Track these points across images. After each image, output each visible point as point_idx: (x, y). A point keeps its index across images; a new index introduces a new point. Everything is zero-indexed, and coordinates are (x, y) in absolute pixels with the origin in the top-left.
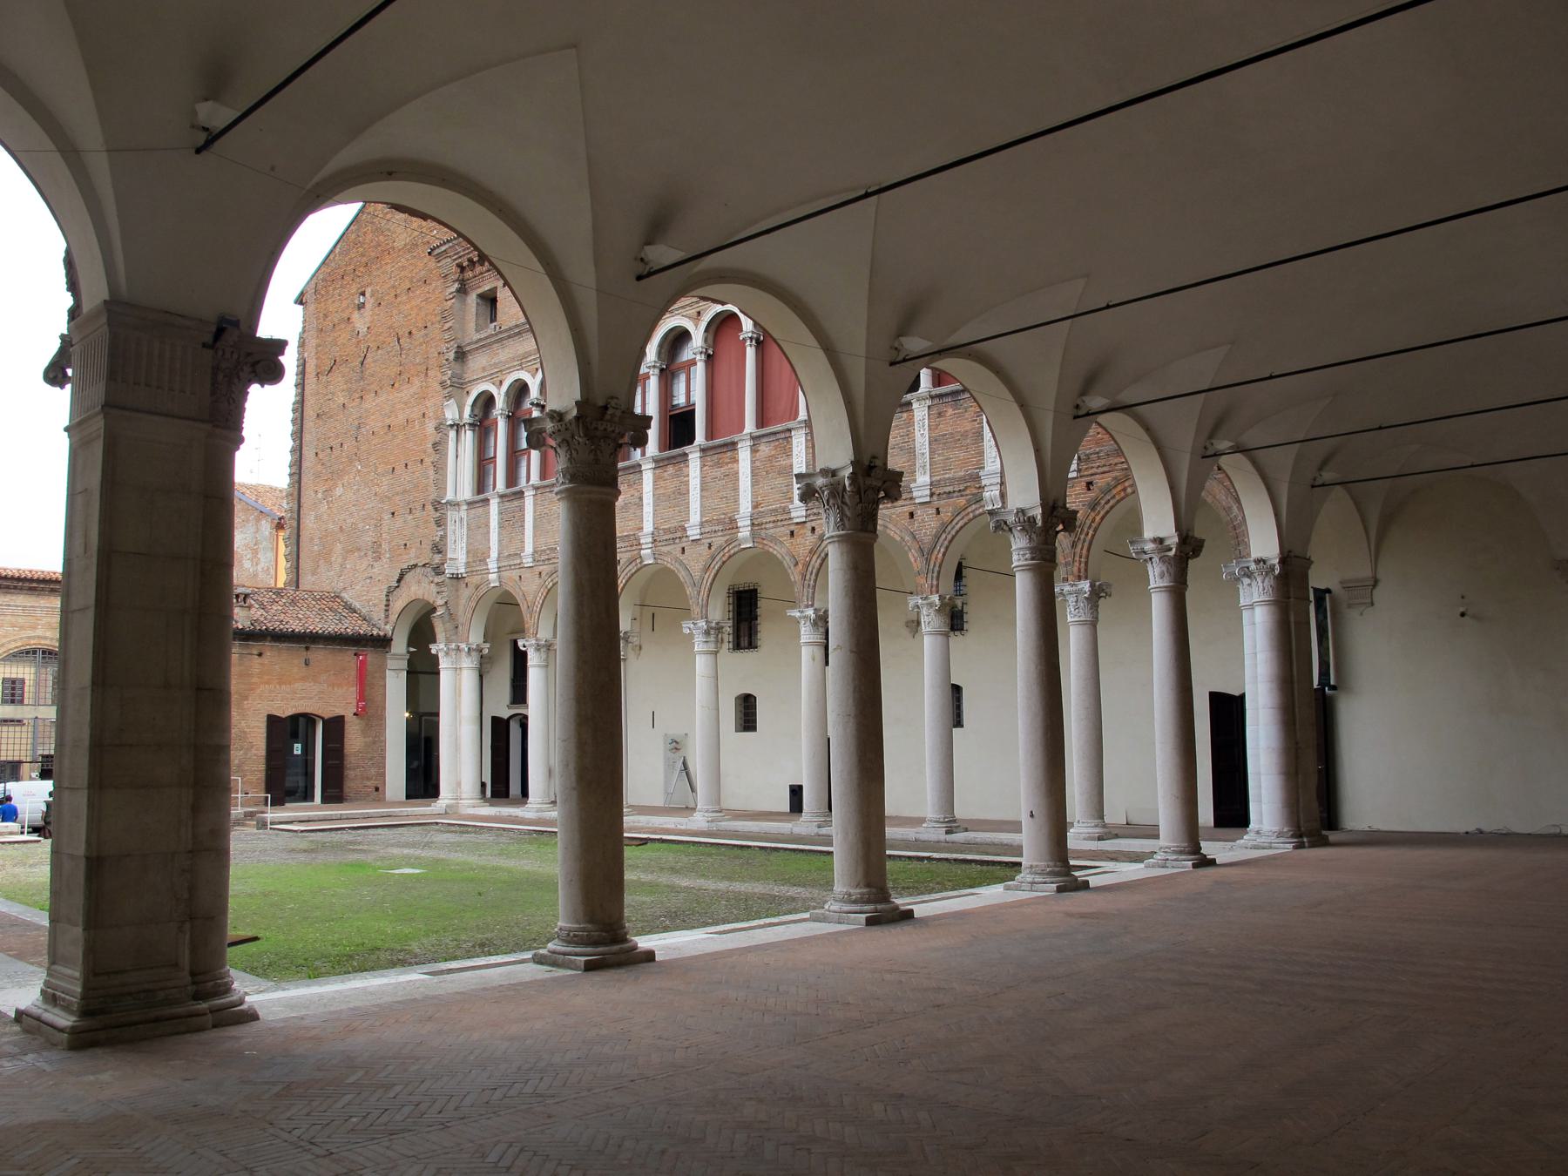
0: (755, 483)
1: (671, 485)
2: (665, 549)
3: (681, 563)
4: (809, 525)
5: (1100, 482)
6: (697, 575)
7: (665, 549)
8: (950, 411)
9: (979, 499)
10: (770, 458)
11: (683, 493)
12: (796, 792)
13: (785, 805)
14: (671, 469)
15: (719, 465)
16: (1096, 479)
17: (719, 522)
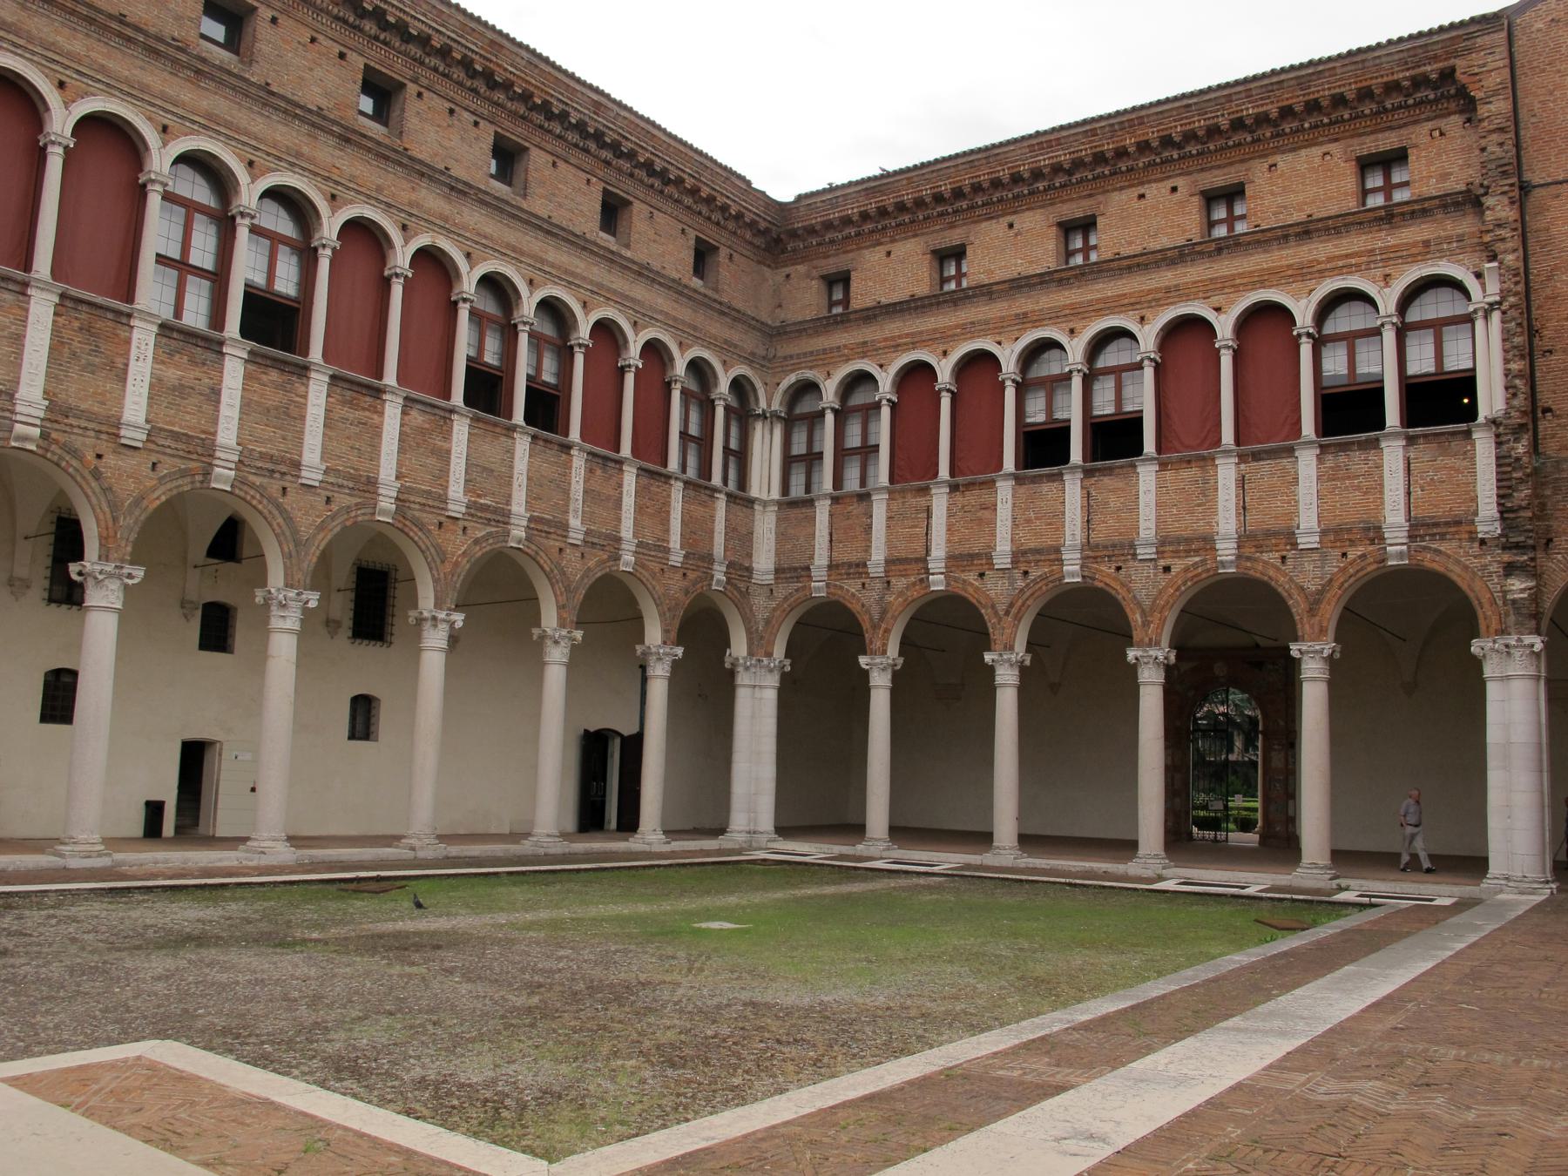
0: (401, 450)
1: (274, 398)
2: (258, 481)
3: (278, 506)
4: (461, 523)
5: (691, 575)
6: (305, 531)
7: (258, 481)
8: (599, 472)
9: (617, 558)
10: (421, 431)
11: (293, 416)
12: (154, 810)
13: (138, 829)
14: (274, 375)
15: (352, 404)
16: (689, 573)
17: (352, 478)
